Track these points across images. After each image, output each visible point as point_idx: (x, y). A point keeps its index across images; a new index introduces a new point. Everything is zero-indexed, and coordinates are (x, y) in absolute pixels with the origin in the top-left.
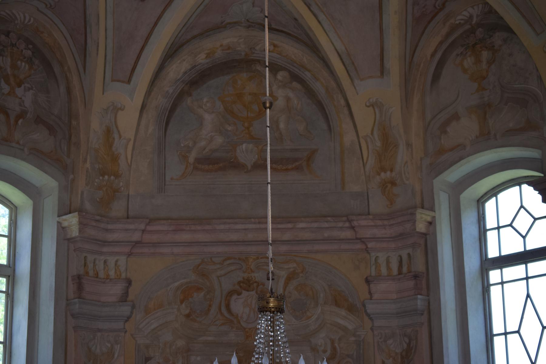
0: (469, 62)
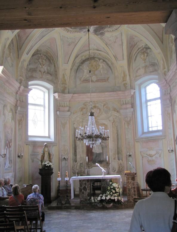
0: (142, 56)
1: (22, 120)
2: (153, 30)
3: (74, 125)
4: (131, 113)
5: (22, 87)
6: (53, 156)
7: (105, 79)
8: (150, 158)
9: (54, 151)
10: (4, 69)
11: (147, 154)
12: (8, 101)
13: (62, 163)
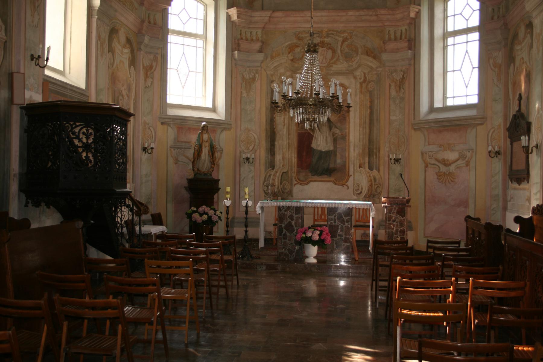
1: (154, 68)
6: (221, 153)
8: (443, 169)
9: (223, 140)
11: (436, 160)
12: (122, 19)
13: (242, 170)
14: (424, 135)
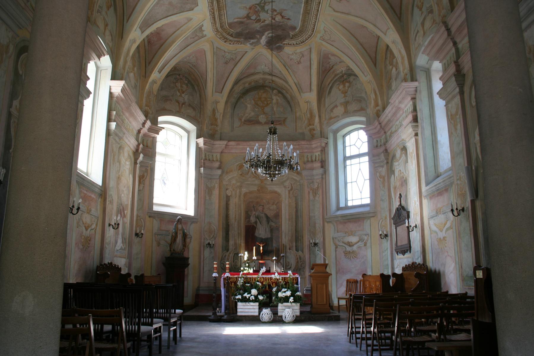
0: (341, 87)
2: (361, 45)
3: (227, 191)
4: (321, 176)
5: (148, 124)
6: (191, 240)
7: (279, 121)
8: (349, 249)
9: (192, 230)
10: (126, 86)
11: (343, 242)
12: (127, 141)
14: (334, 226)
